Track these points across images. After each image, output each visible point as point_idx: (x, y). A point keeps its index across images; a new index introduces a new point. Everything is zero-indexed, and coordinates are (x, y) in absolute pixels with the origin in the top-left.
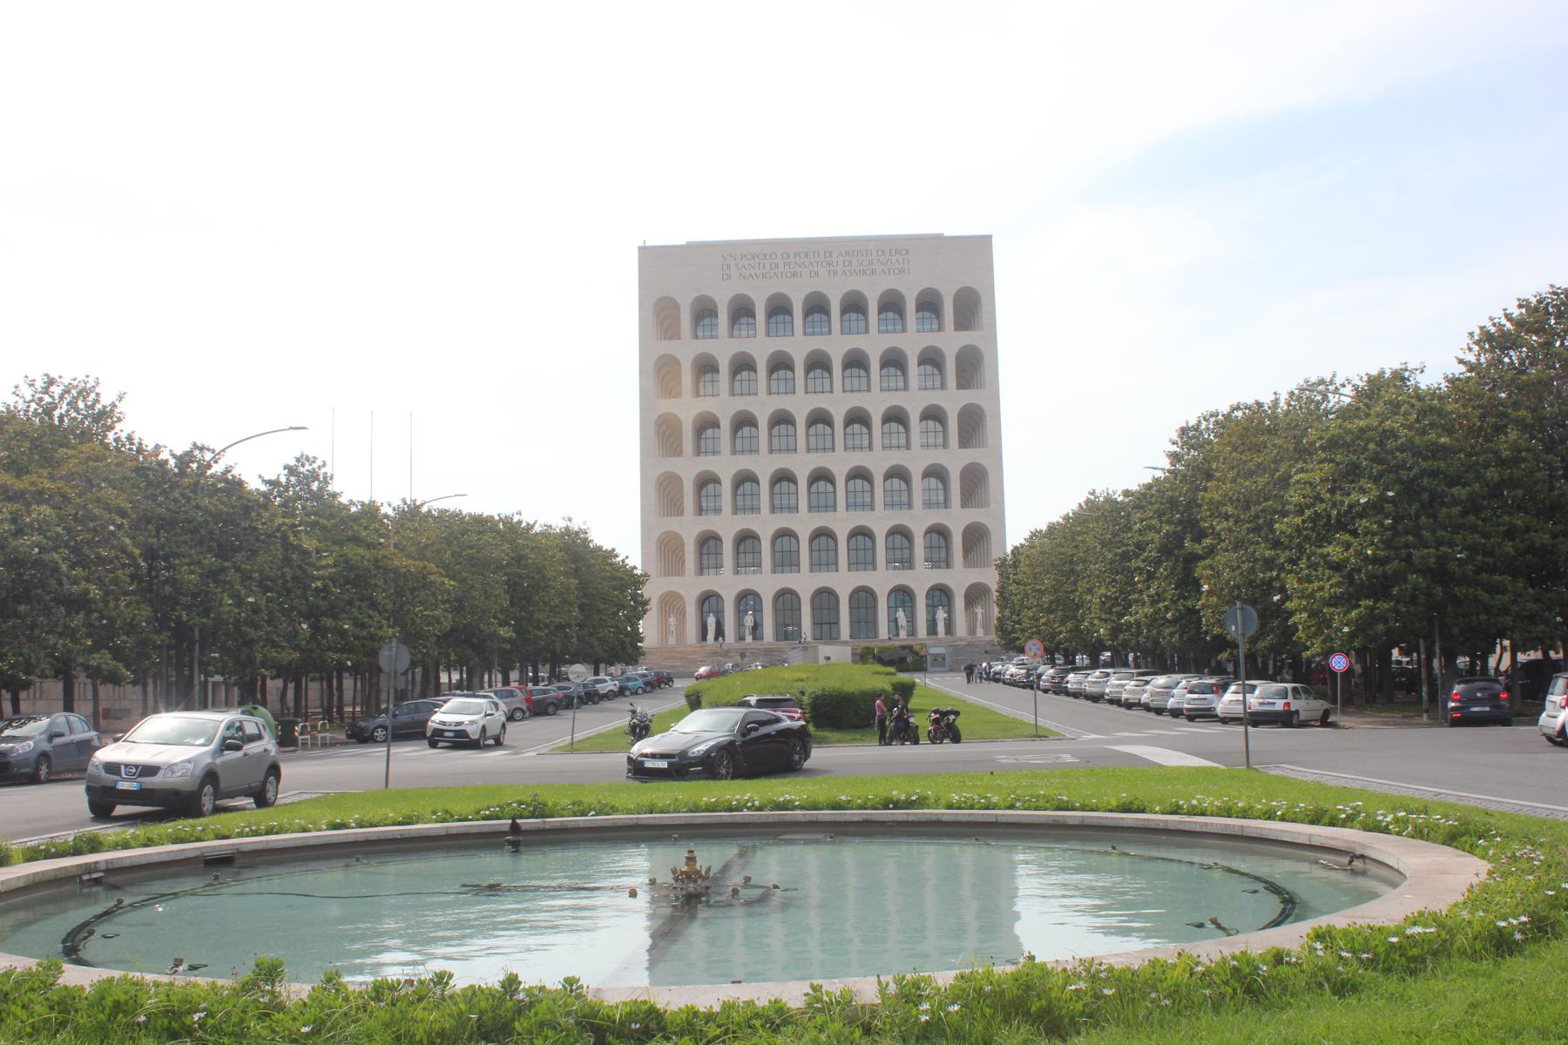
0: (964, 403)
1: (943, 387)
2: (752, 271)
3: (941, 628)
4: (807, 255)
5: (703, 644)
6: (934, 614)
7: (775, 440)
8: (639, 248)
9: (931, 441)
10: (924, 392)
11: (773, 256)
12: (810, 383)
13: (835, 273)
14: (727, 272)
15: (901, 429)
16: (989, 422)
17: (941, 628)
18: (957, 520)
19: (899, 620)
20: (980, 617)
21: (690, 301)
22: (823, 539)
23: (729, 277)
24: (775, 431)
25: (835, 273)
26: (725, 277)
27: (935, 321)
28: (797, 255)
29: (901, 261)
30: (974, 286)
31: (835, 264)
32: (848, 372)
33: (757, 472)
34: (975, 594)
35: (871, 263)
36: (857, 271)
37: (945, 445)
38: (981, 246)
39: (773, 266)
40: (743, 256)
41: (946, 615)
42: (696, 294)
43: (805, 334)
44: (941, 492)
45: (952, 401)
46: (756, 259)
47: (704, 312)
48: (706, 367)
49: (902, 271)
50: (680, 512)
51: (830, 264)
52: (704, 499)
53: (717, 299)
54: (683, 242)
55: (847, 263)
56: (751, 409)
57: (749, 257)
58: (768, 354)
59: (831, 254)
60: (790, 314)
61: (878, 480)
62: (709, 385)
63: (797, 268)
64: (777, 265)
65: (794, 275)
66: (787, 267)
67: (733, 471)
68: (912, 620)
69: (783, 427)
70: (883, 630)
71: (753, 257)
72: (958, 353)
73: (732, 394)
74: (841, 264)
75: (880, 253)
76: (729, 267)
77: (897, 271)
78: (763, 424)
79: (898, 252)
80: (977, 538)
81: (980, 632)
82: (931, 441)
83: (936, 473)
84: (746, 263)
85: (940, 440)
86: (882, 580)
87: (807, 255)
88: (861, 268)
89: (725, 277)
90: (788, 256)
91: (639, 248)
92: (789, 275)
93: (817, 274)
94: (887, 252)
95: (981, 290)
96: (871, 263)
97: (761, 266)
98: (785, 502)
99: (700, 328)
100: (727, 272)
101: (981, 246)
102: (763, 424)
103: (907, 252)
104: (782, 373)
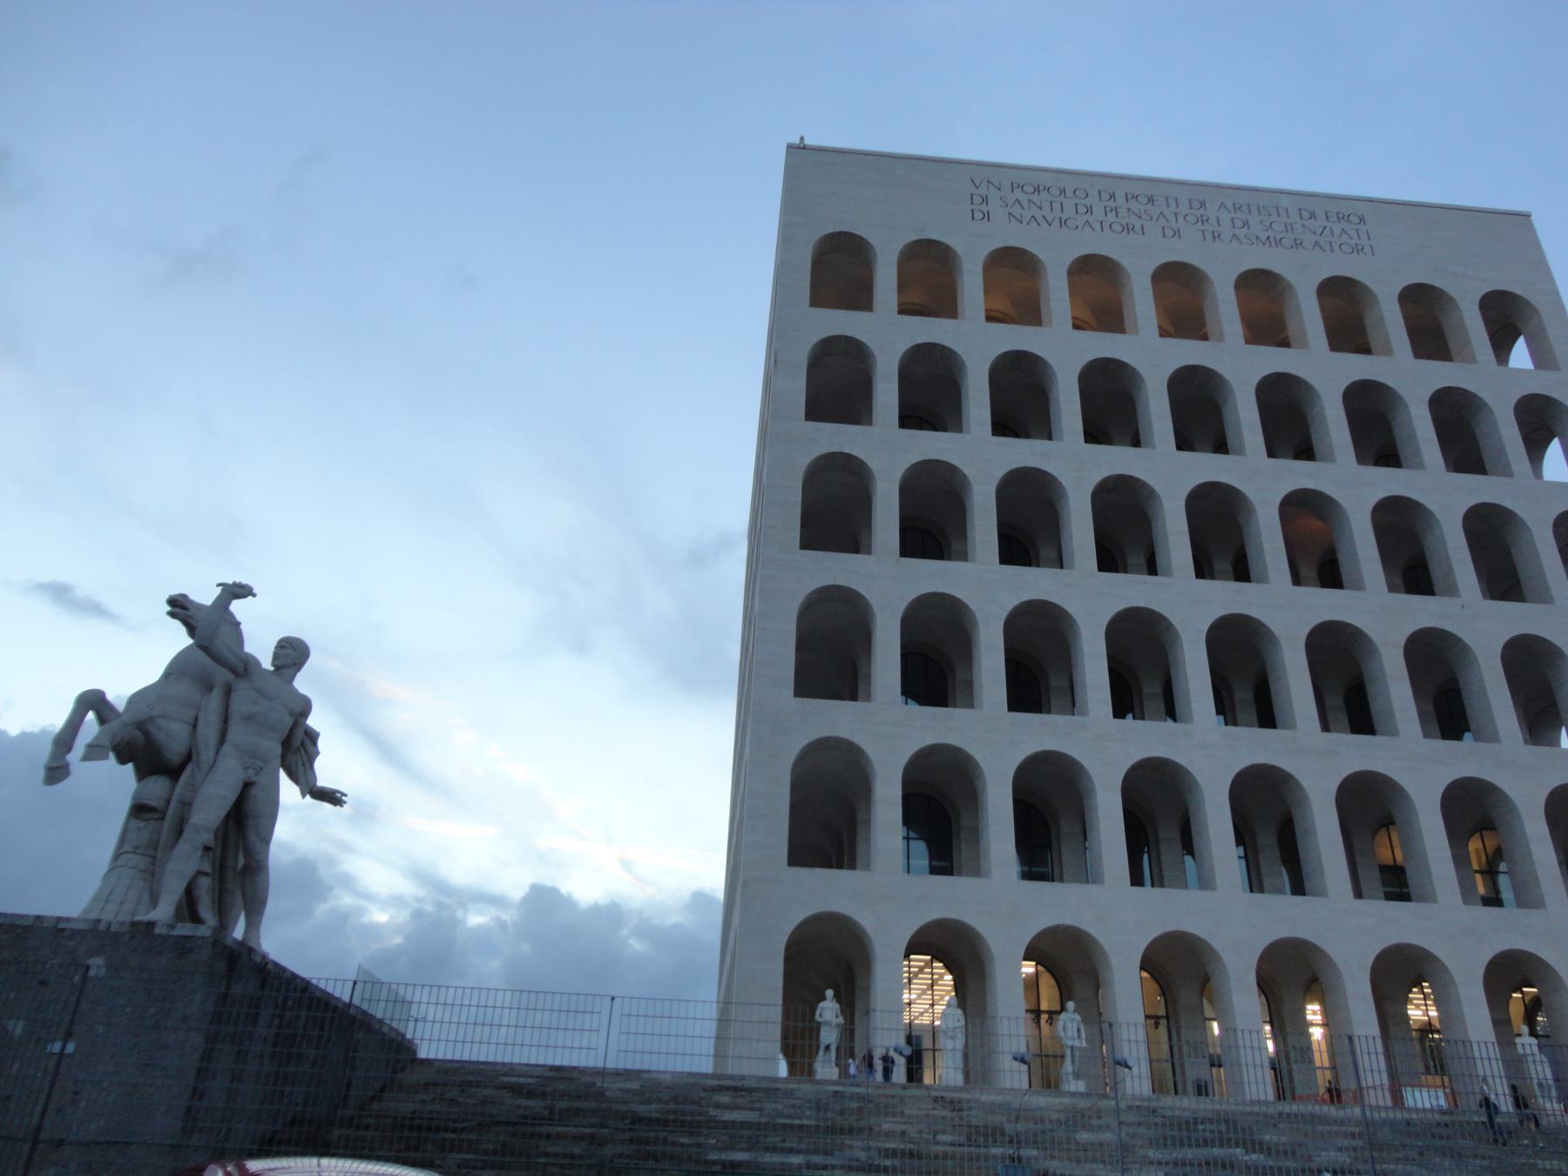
2: (1037, 214)
4: (1151, 200)
8: (790, 147)
11: (1081, 194)
14: (984, 208)
21: (899, 245)
23: (987, 216)
25: (1216, 237)
26: (978, 215)
29: (1354, 234)
31: (1213, 220)
35: (1288, 228)
36: (1263, 238)
39: (1082, 210)
42: (914, 237)
46: (1044, 194)
49: (1357, 249)
51: (1203, 220)
55: (1239, 224)
57: (1029, 189)
59: (1202, 204)
64: (1089, 210)
65: (1128, 229)
66: (1111, 216)
71: (1037, 190)
75: (1306, 215)
76: (985, 200)
77: (1347, 248)
79: (1341, 217)
84: (1024, 198)
88: (1270, 233)
89: (978, 215)
90: (1113, 196)
91: (790, 147)
92: (1117, 228)
93: (1177, 233)
96: (1288, 228)
97: (1057, 206)
100: (984, 208)
103: (1362, 220)
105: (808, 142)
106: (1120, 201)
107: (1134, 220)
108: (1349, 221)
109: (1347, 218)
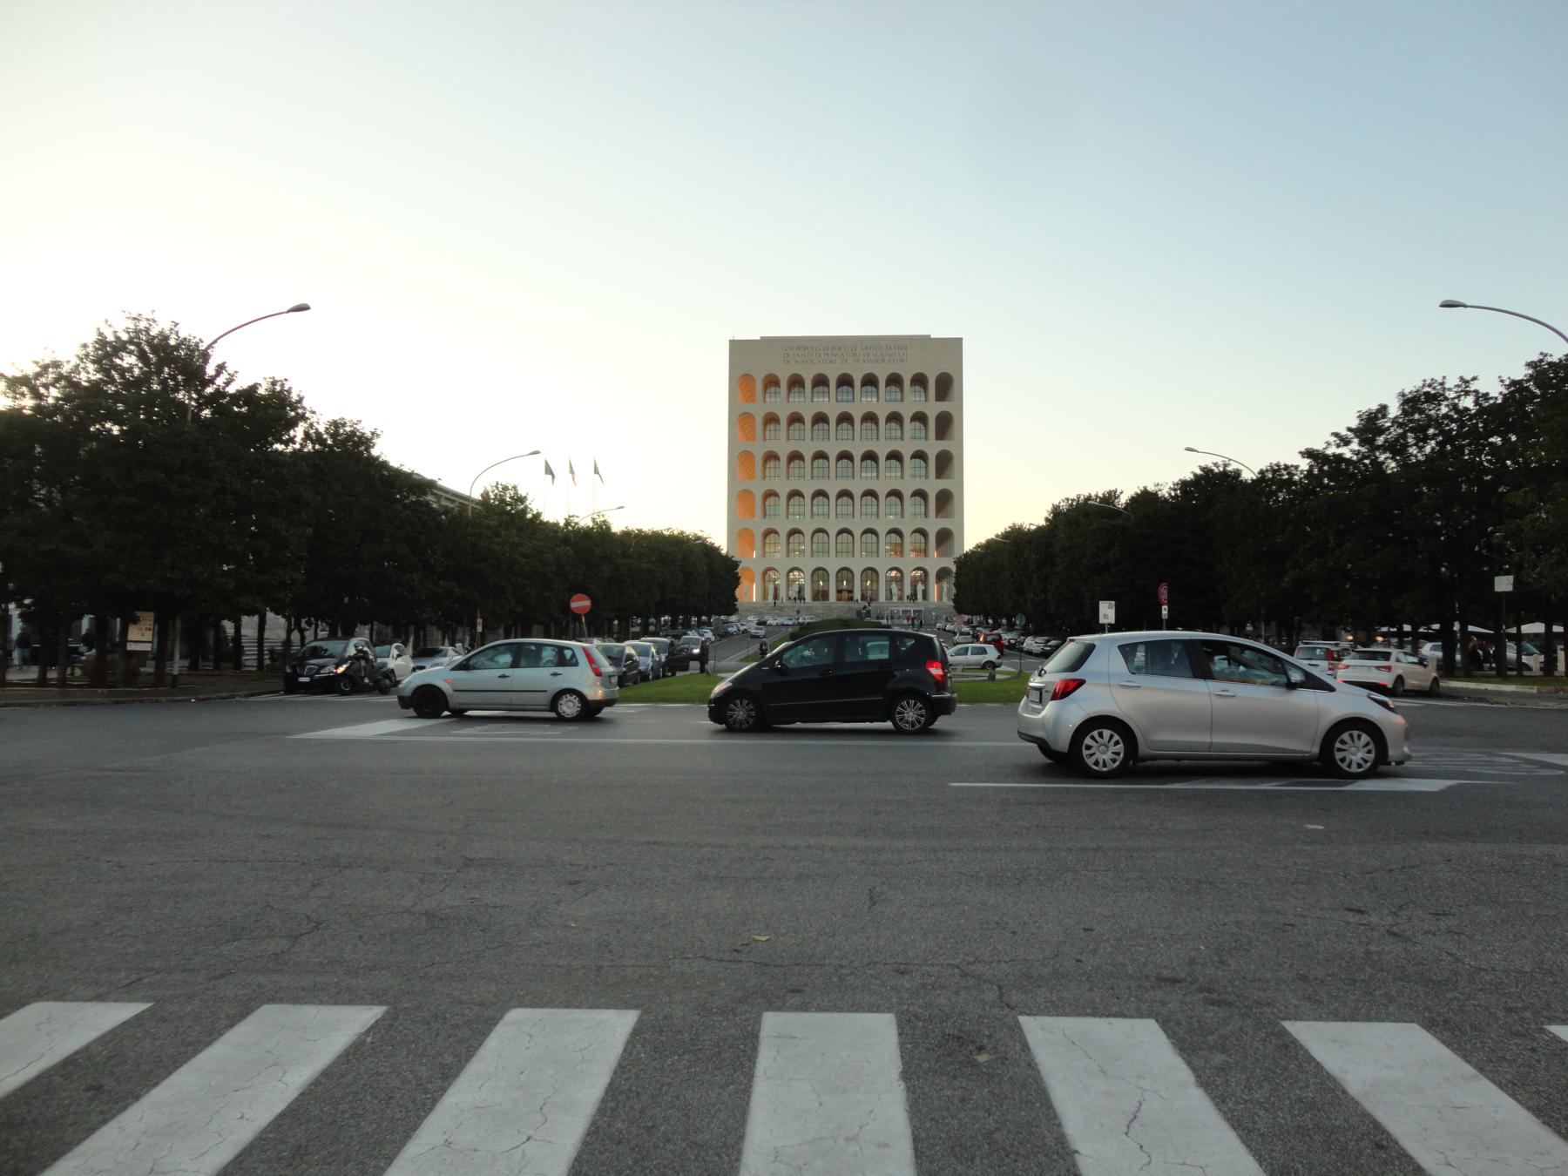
0: (940, 449)
1: (926, 438)
3: (920, 596)
5: (766, 602)
6: (916, 586)
7: (815, 471)
8: (730, 341)
9: (917, 473)
10: (914, 441)
12: (840, 432)
13: (858, 361)
15: (898, 464)
16: (955, 461)
17: (920, 596)
18: (933, 525)
19: (893, 590)
20: (945, 589)
22: (845, 535)
23: (789, 362)
24: (816, 462)
25: (858, 361)
27: (923, 393)
28: (833, 348)
30: (949, 371)
32: (864, 425)
33: (804, 491)
34: (942, 574)
37: (927, 477)
38: (956, 344)
40: (798, 348)
41: (923, 588)
42: (767, 373)
43: (837, 401)
44: (923, 507)
45: (933, 448)
46: (807, 351)
47: (771, 382)
48: (771, 419)
49: (902, 361)
50: (752, 515)
51: (855, 355)
52: (768, 508)
53: (780, 377)
54: (759, 338)
56: (801, 450)
58: (813, 413)
60: (828, 386)
61: (882, 497)
62: (772, 433)
63: (834, 358)
64: (820, 355)
65: (831, 362)
67: (788, 490)
68: (901, 590)
69: (821, 461)
70: (882, 597)
72: (940, 414)
73: (788, 439)
74: (862, 356)
76: (788, 355)
78: (808, 458)
79: (900, 348)
80: (945, 537)
81: (945, 599)
82: (917, 473)
83: (921, 494)
85: (923, 473)
86: (883, 563)
87: (840, 348)
91: (730, 341)
93: (846, 361)
94: (892, 348)
95: (954, 376)
98: (821, 511)
99: (767, 395)
101: (956, 344)
102: (808, 458)
103: (906, 348)
104: (821, 425)
105: (735, 339)
106: (830, 349)
107: (834, 358)
108: (901, 349)
109: (900, 348)
